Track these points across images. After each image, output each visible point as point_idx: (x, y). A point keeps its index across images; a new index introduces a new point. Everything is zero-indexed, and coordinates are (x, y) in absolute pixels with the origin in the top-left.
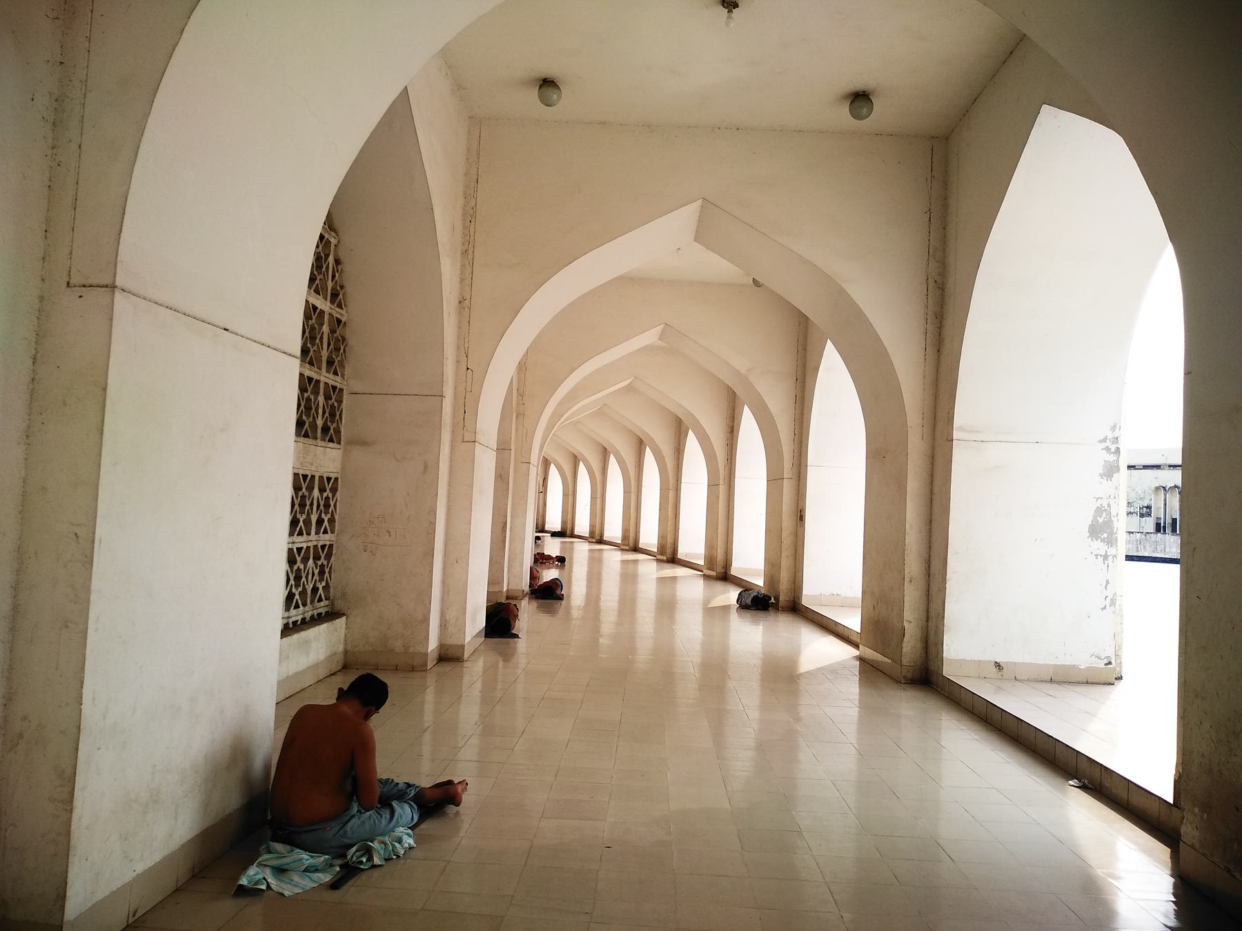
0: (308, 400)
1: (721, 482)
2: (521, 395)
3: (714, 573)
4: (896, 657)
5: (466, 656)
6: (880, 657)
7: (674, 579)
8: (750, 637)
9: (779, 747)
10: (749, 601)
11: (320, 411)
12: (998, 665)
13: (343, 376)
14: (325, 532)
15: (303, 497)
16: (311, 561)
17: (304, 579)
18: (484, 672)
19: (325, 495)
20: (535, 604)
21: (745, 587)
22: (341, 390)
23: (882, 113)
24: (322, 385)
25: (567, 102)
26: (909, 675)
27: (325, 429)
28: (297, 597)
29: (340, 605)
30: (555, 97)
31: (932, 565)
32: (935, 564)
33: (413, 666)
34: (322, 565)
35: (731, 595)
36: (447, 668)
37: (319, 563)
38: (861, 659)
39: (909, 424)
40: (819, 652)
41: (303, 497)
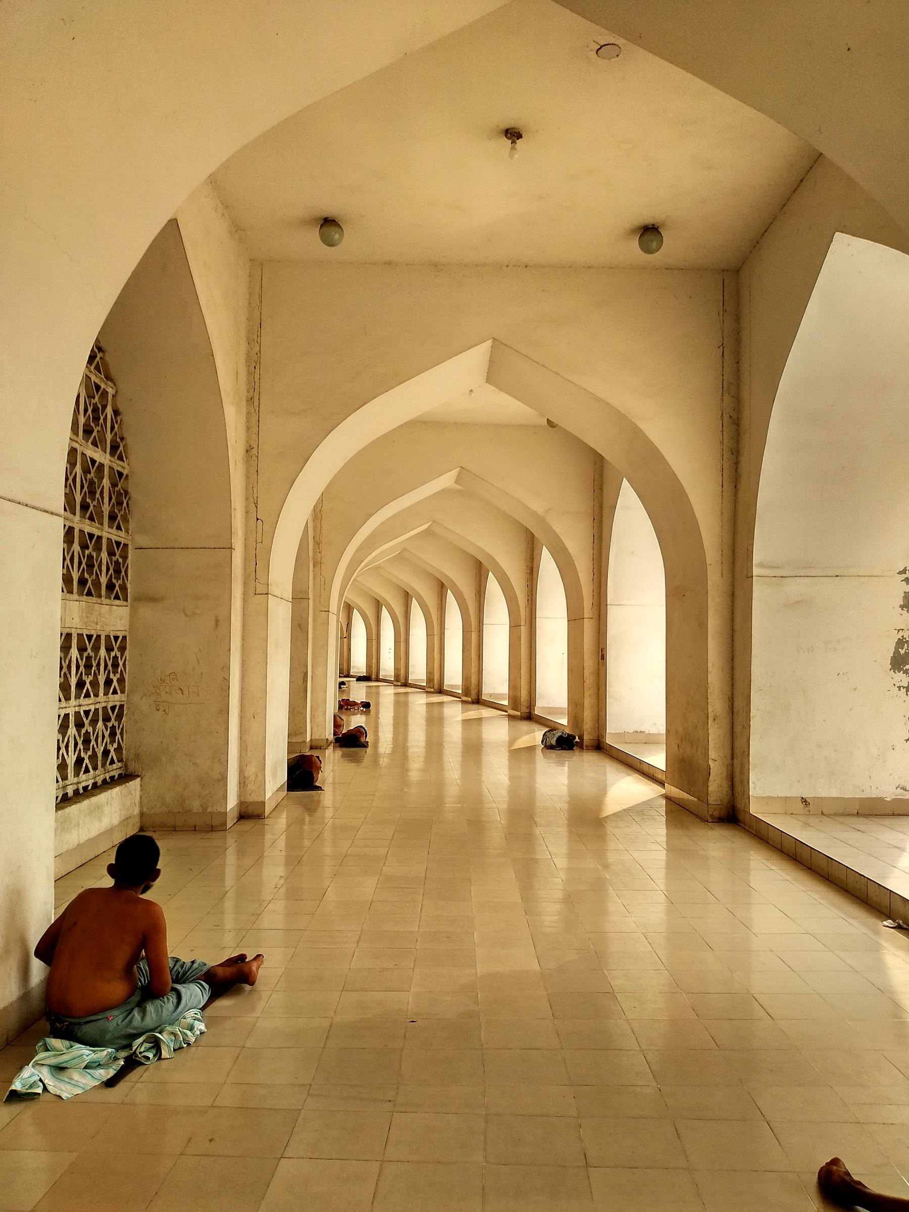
0: (90, 557)
1: (523, 623)
4: (702, 797)
6: (686, 796)
9: (589, 895)
11: (104, 568)
13: (127, 531)
14: (115, 692)
15: (89, 658)
16: (100, 724)
17: (93, 742)
19: (113, 654)
22: (126, 545)
24: (104, 541)
26: (716, 814)
27: (110, 587)
28: (87, 761)
29: (133, 767)
33: (210, 826)
34: (113, 727)
37: (110, 725)
38: (668, 798)
41: (89, 658)
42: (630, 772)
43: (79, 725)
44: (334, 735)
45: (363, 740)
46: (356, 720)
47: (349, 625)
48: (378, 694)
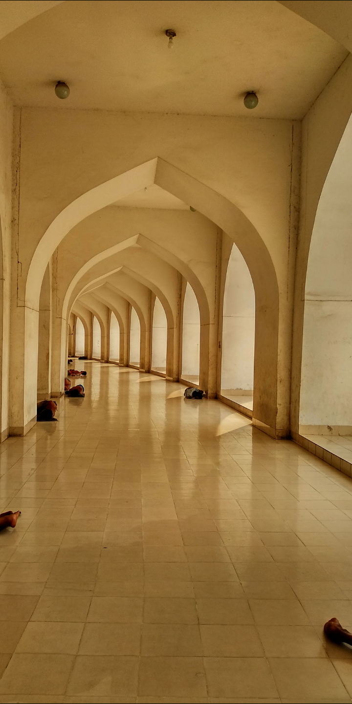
1: (175, 326)
2: (55, 277)
3: (172, 379)
4: (273, 425)
5: (25, 433)
6: (263, 425)
7: (149, 382)
8: (192, 415)
9: (209, 478)
10: (191, 394)
12: (329, 428)
18: (37, 441)
20: (68, 400)
21: (190, 386)
26: (280, 435)
30: (66, 92)
31: (293, 373)
32: (294, 372)
35: (181, 391)
36: (13, 440)
38: (253, 426)
39: (280, 292)
40: (231, 421)
42: (233, 411)
44: (65, 390)
45: (81, 393)
46: (79, 382)
47: (74, 326)
48: (91, 367)
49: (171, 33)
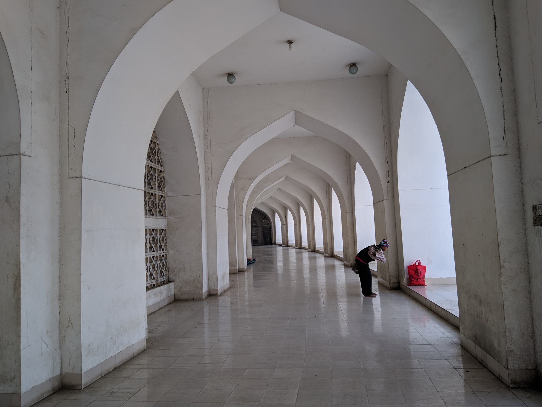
0: (152, 202)
23: (361, 70)
25: (238, 80)
27: (160, 212)
43: (151, 262)
49: (290, 42)
